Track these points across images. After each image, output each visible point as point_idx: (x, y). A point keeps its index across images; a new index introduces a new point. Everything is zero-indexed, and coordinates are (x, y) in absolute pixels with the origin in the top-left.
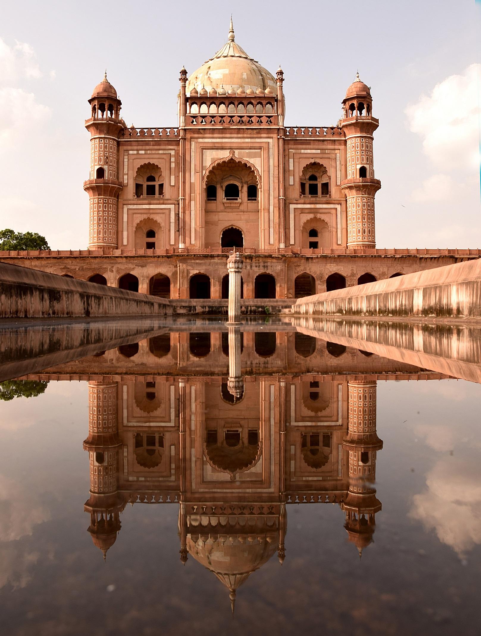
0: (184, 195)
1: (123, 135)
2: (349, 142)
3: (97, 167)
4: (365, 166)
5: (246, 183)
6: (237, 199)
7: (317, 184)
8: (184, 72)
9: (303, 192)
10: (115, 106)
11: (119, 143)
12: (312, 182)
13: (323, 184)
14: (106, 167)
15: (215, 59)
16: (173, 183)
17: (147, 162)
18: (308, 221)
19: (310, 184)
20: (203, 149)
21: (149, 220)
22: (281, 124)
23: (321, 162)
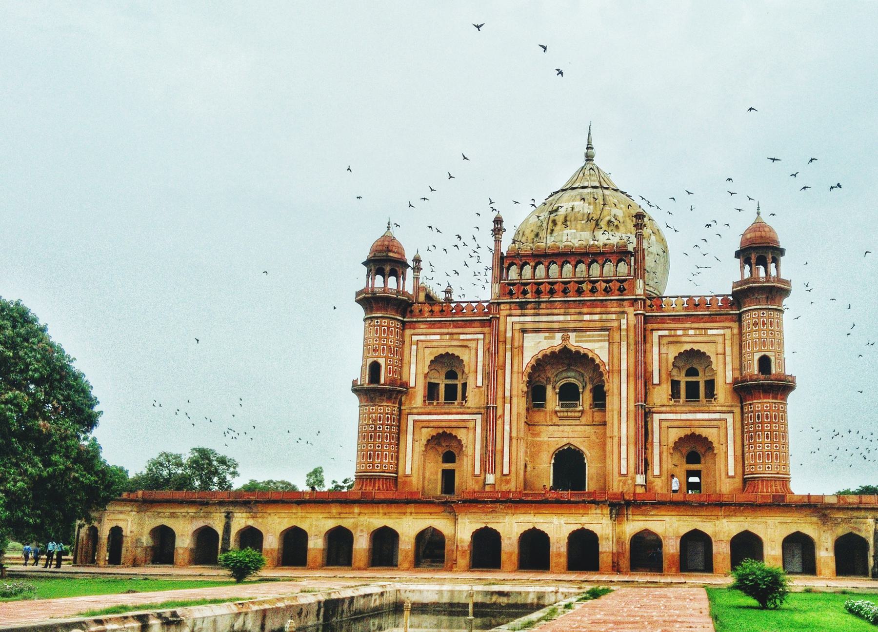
0: (495, 400)
1: (411, 311)
3: (370, 361)
4: (767, 354)
5: (592, 380)
8: (498, 221)
9: (675, 394)
10: (400, 271)
13: (706, 382)
14: (382, 361)
16: (479, 384)
17: (442, 351)
18: (680, 439)
20: (524, 331)
22: (640, 291)
23: (703, 348)
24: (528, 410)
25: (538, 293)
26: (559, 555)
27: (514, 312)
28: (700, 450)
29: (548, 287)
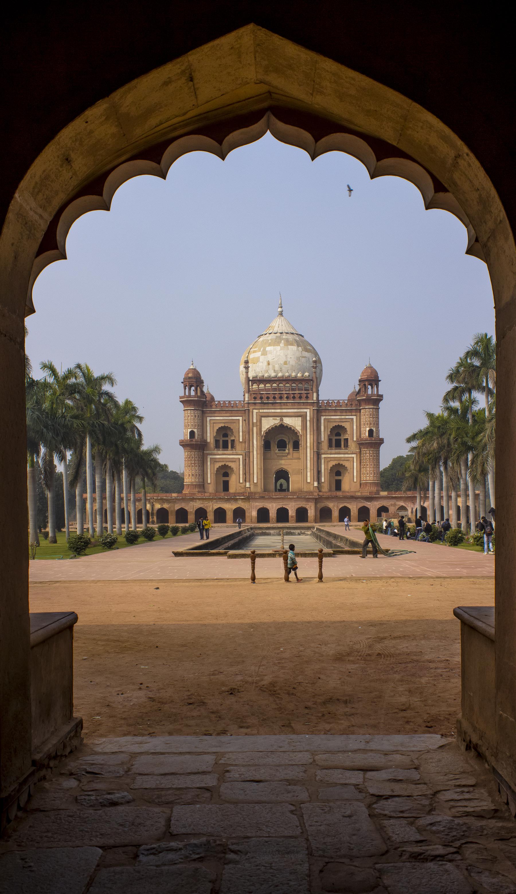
0: (249, 449)
1: (206, 406)
2: (362, 411)
3: (189, 430)
6: (285, 450)
7: (340, 439)
9: (330, 446)
11: (203, 412)
12: (338, 438)
13: (345, 439)
14: (195, 430)
15: (268, 334)
16: (241, 440)
17: (223, 425)
18: (333, 466)
19: (336, 439)
20: (262, 417)
21: (225, 467)
23: (343, 424)
24: (264, 453)
25: (268, 398)
26: (292, 517)
27: (256, 407)
28: (341, 470)
29: (273, 396)
